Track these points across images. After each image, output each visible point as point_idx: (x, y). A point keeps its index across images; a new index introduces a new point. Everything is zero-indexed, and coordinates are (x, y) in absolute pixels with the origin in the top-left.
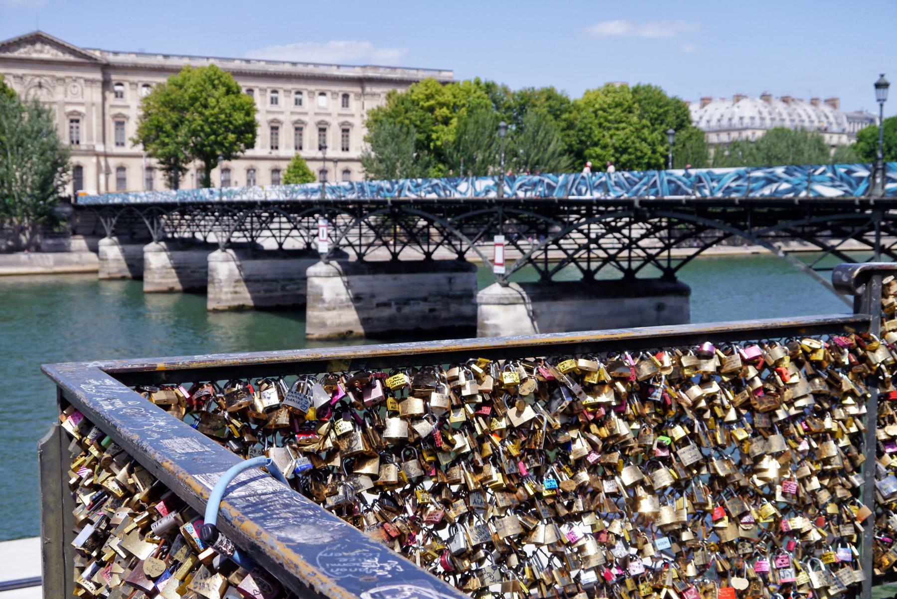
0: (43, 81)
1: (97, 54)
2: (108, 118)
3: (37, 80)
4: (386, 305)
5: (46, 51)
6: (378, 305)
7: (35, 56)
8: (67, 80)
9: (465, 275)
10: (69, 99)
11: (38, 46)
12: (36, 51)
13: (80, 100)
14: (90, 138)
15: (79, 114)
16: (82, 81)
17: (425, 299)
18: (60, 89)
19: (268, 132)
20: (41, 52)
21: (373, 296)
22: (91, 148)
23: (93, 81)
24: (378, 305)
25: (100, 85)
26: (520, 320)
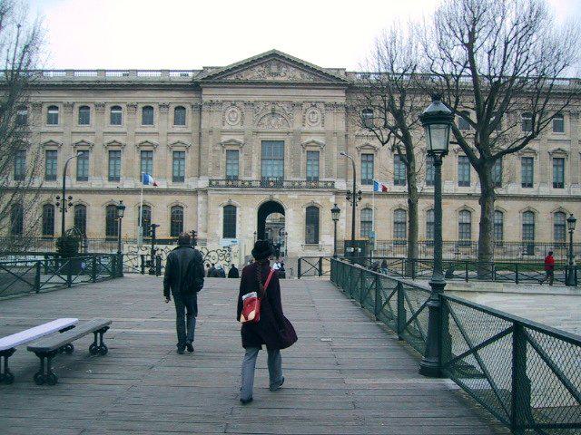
0: (277, 108)
1: (342, 73)
2: (352, 150)
3: (269, 108)
5: (282, 74)
7: (269, 79)
8: (305, 106)
10: (306, 128)
11: (274, 69)
12: (271, 74)
13: (320, 128)
14: (329, 174)
15: (318, 144)
16: (322, 106)
18: (297, 116)
19: (550, 166)
20: (277, 75)
22: (329, 184)
23: (335, 105)
25: (343, 110)
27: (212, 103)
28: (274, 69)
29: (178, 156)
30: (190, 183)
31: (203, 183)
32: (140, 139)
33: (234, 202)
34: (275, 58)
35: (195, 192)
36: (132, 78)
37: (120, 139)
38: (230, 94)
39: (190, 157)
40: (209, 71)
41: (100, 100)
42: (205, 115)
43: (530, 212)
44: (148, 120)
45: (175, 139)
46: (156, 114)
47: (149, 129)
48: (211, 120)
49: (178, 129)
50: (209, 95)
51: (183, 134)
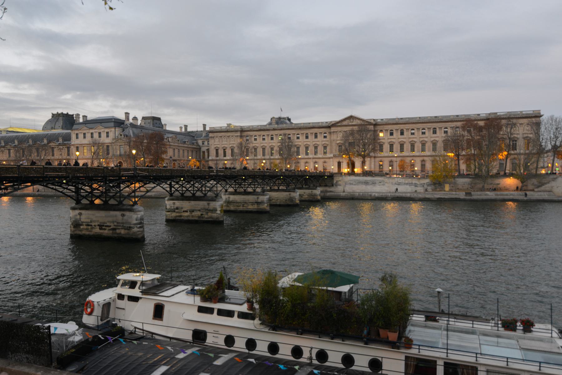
4: (186, 211)
6: (184, 211)
7: (350, 124)
9: (214, 203)
11: (352, 120)
17: (199, 210)
21: (182, 208)
24: (184, 211)
26: (76, 216)
27: (334, 132)
28: (352, 120)
29: (325, 147)
30: (329, 155)
31: (332, 155)
32: (314, 143)
33: (341, 161)
34: (351, 117)
35: (330, 158)
36: (311, 125)
37: (308, 143)
38: (339, 129)
39: (328, 148)
40: (333, 123)
41: (302, 132)
42: (332, 135)
43: (423, 161)
44: (316, 137)
45: (324, 143)
46: (318, 135)
47: (316, 140)
48: (334, 137)
49: (325, 139)
50: (333, 129)
51: (326, 141)
